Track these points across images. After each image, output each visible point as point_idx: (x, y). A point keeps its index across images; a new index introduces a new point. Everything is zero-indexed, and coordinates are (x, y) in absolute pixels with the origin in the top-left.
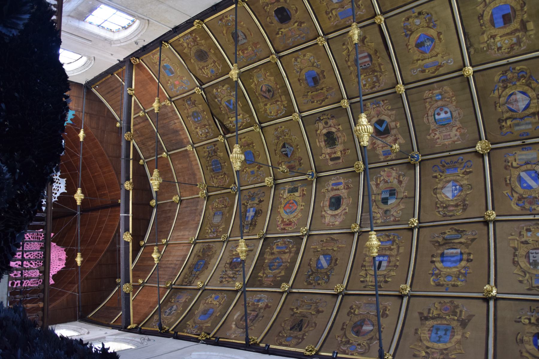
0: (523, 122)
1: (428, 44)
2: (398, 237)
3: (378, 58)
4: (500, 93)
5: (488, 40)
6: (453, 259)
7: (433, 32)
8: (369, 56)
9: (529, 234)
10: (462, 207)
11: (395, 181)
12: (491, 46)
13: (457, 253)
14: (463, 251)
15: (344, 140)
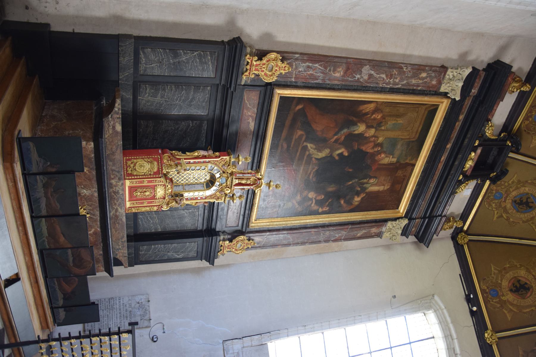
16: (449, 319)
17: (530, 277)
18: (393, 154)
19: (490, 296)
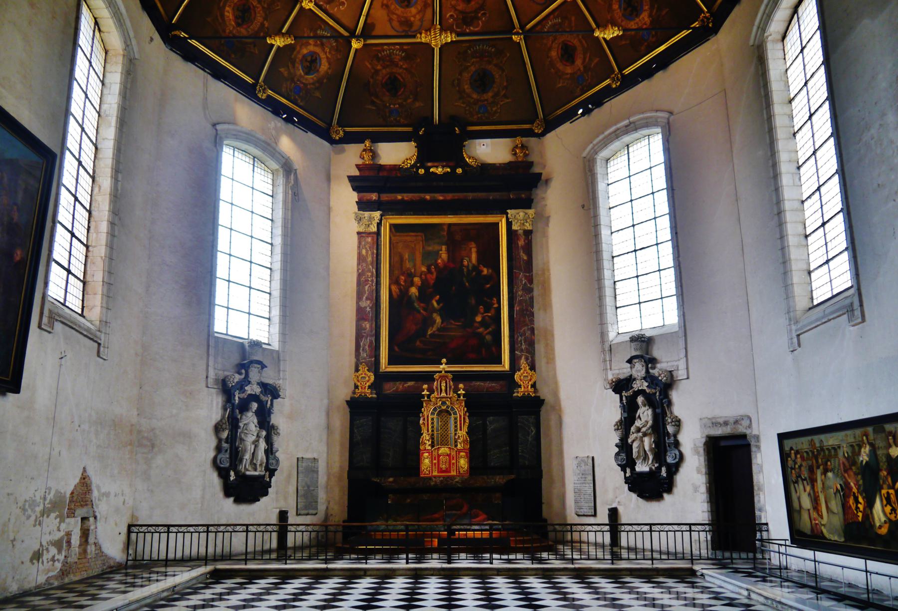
16: (601, 137)
17: (555, 45)
18: (438, 251)
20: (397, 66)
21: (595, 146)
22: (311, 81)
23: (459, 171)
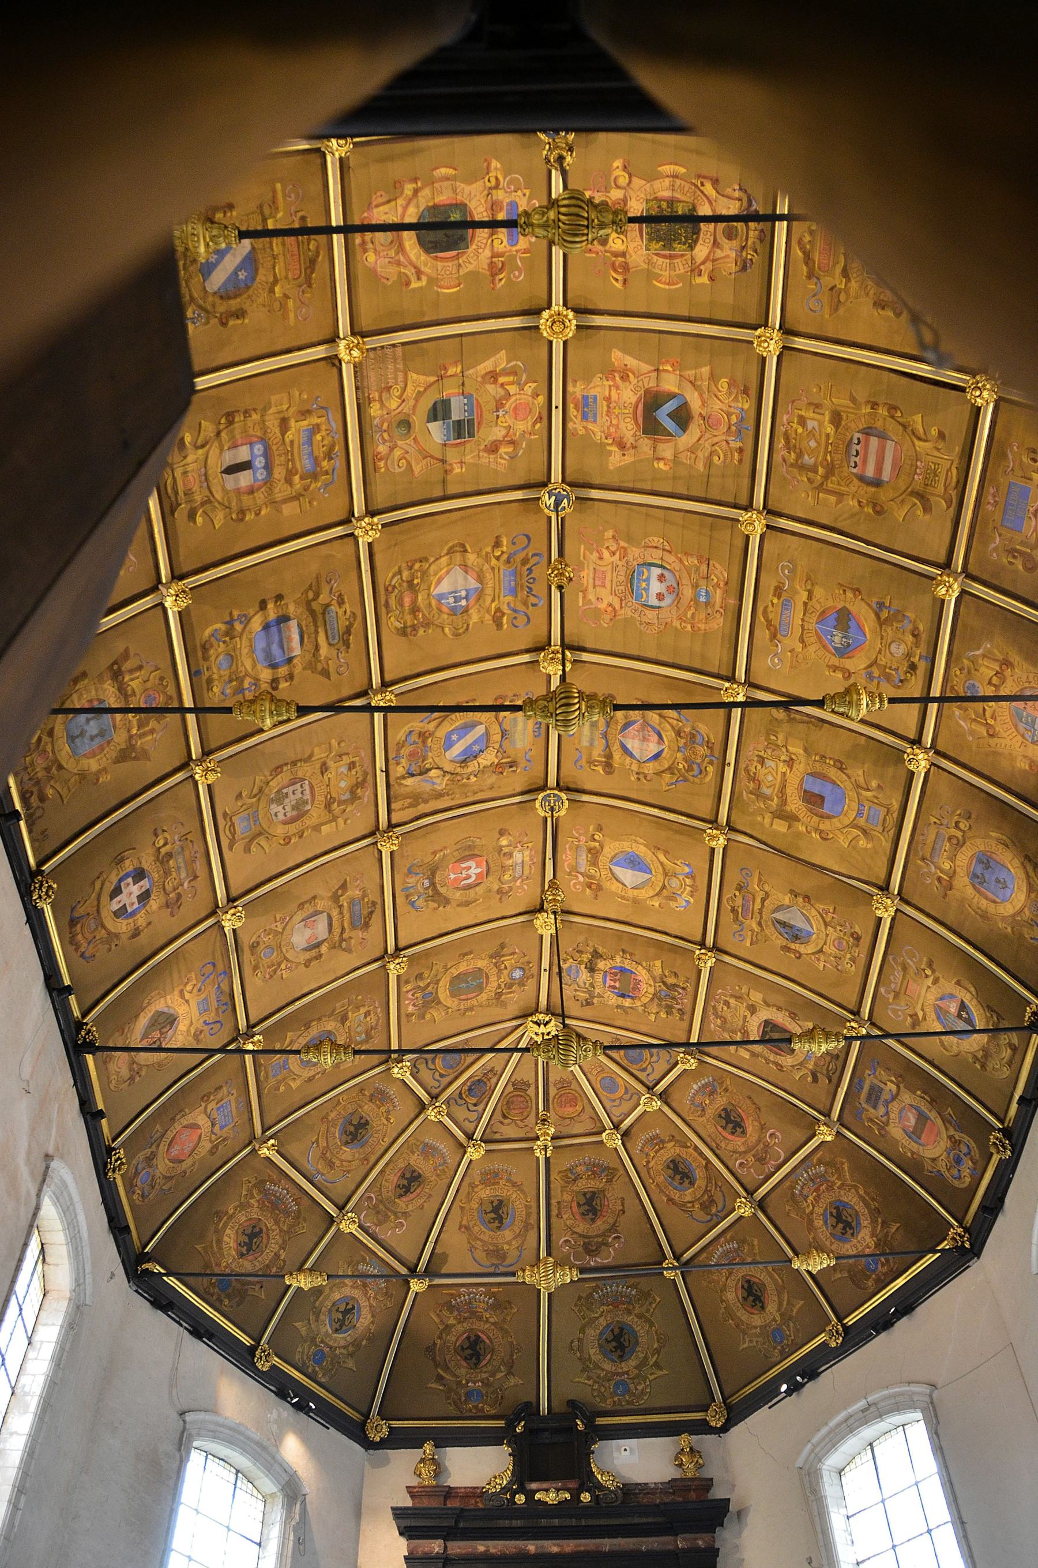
0: (598, 735)
1: (837, 639)
2: (326, 486)
3: (859, 502)
4: (671, 721)
5: (787, 751)
6: (275, 649)
7: (857, 663)
8: (877, 483)
9: (344, 770)
10: (409, 624)
11: (498, 433)
12: (774, 750)
13: (290, 650)
14: (295, 661)
15: (657, 278)
16: (824, 1431)
19: (785, 1342)
20: (480, 1318)
21: (815, 1446)
22: (342, 1343)
23: (585, 1497)
